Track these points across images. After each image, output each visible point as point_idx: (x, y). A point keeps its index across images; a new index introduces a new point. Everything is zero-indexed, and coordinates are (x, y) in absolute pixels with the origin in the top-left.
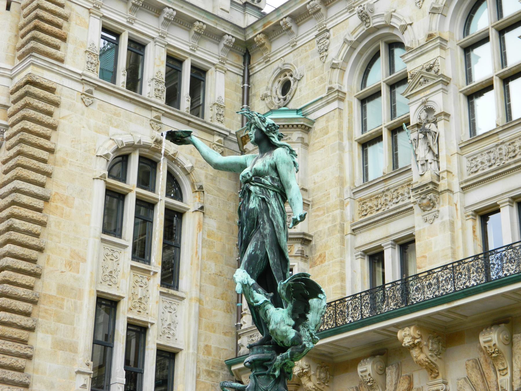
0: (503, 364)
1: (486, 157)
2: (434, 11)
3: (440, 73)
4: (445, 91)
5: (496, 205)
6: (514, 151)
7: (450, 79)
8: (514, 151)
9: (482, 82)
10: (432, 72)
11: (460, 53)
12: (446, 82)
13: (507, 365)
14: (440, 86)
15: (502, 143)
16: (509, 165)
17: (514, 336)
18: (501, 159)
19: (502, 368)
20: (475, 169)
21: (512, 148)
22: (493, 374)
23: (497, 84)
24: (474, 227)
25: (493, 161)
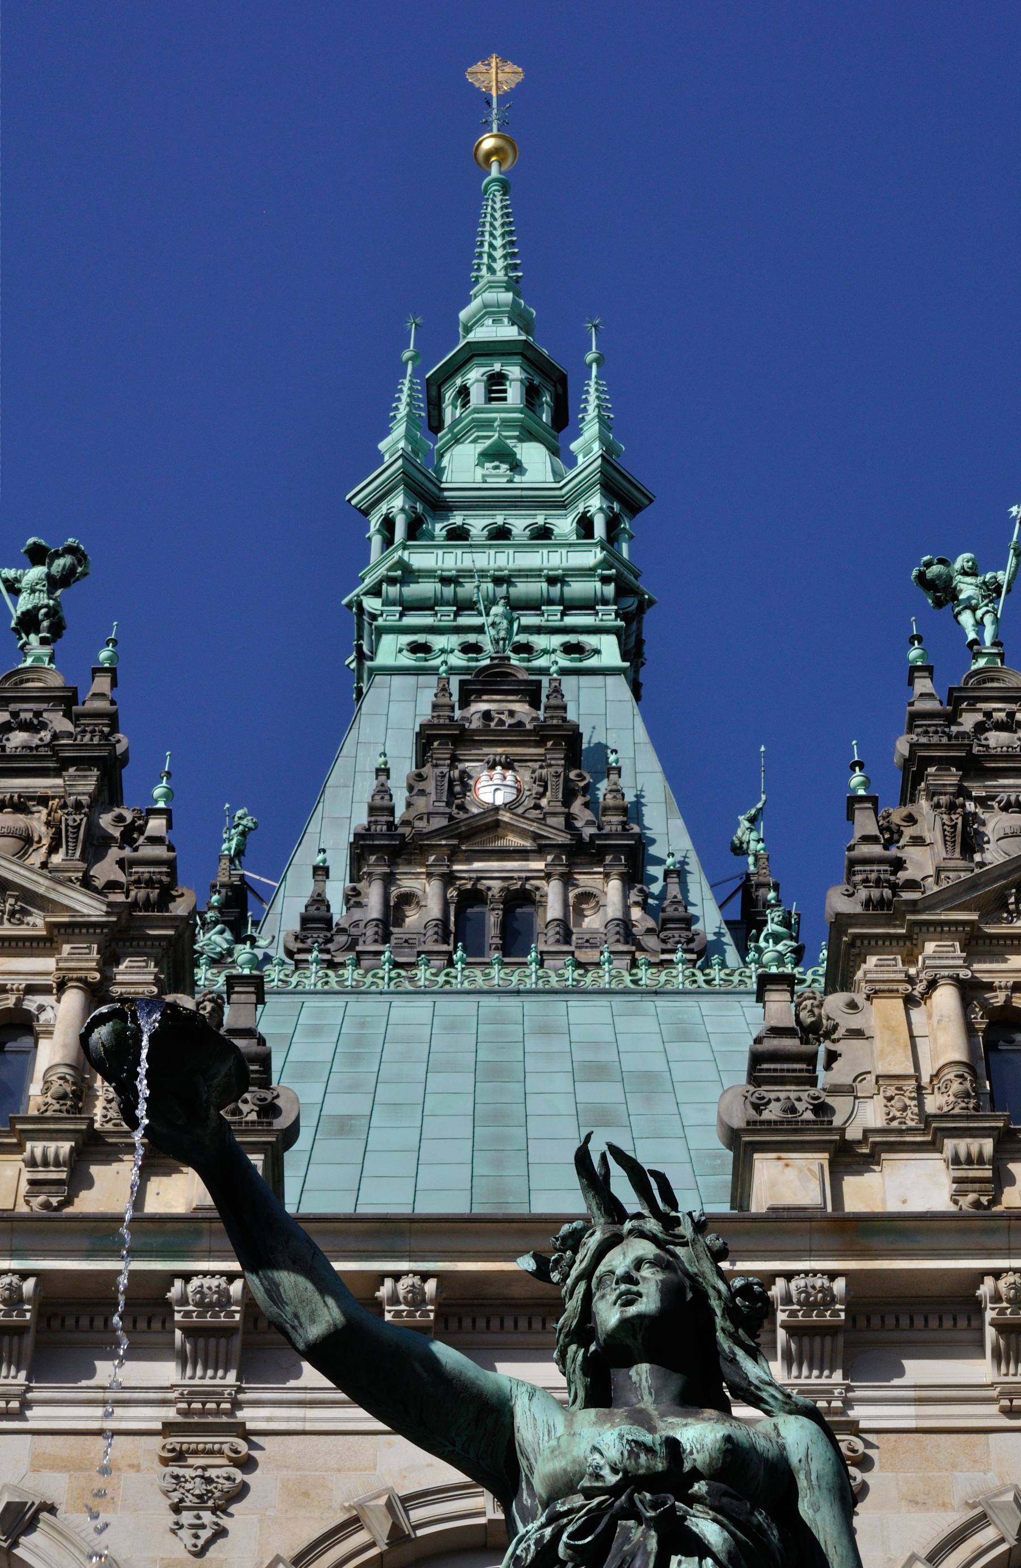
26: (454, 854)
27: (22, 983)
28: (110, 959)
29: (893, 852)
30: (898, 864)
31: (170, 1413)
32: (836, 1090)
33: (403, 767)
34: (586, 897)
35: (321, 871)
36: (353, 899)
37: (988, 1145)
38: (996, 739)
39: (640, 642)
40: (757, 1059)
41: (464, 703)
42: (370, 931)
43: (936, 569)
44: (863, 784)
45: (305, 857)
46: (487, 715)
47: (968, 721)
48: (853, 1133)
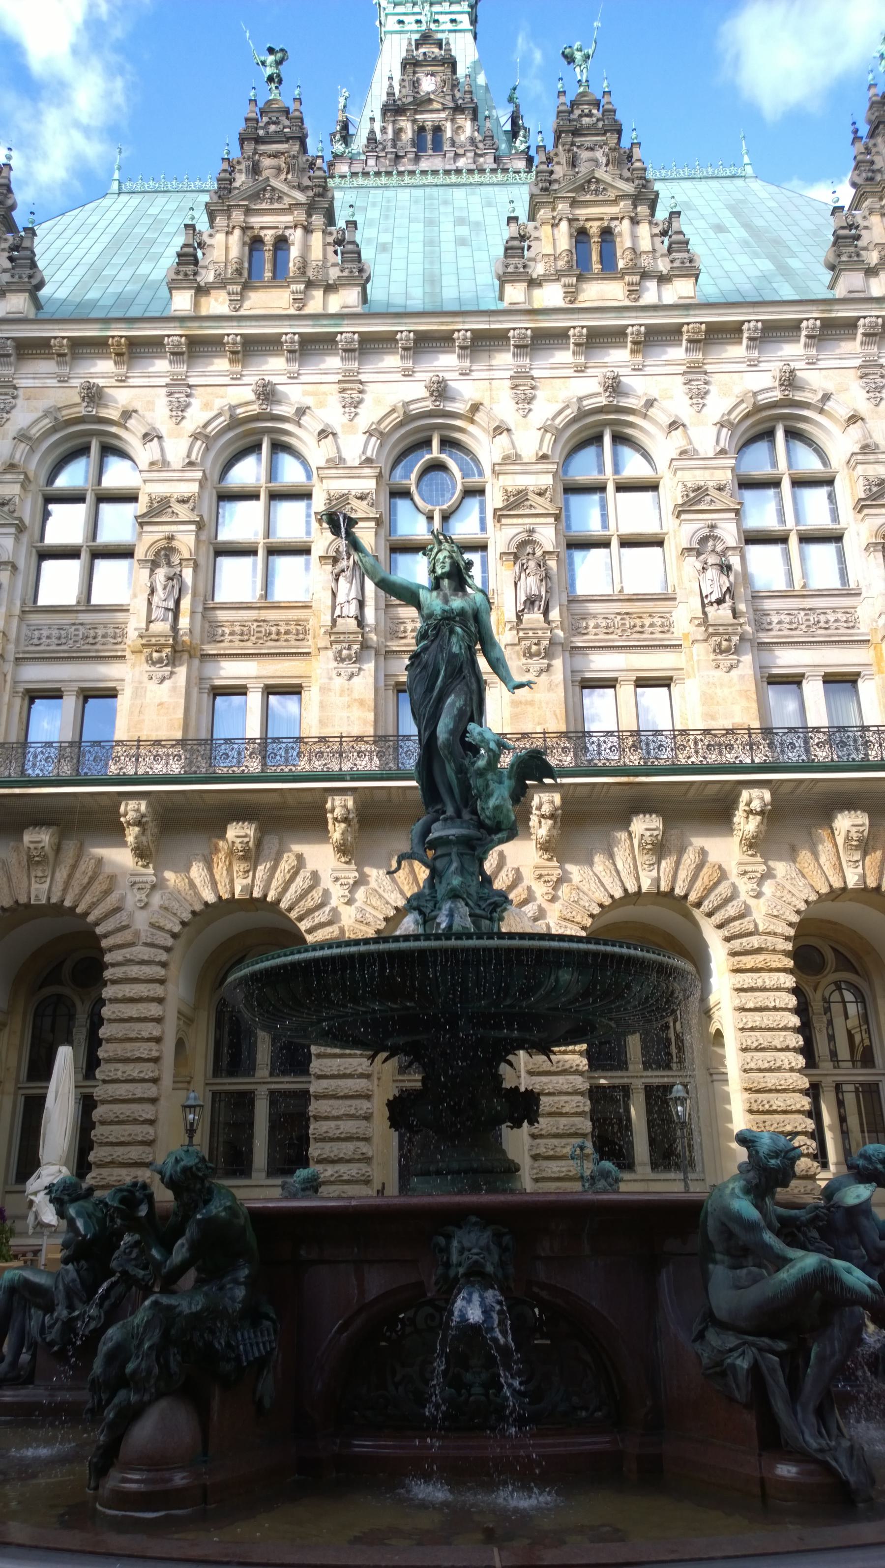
0: (43, 871)
1: (55, 633)
2: (22, 437)
3: (15, 515)
4: (17, 539)
5: (59, 690)
6: (95, 638)
7: (26, 528)
8: (95, 638)
9: (66, 546)
10: (6, 509)
11: (40, 501)
12: (21, 528)
13: (48, 873)
14: (12, 530)
15: (82, 624)
16: (89, 651)
17: (64, 842)
18: (75, 641)
19: (40, 874)
20: (36, 641)
21: (92, 633)
22: (25, 879)
23: (84, 555)
24: (21, 708)
25: (64, 641)
26: (416, 112)
27: (283, 225)
28: (309, 215)
29: (550, 168)
30: (552, 172)
31: (340, 377)
32: (530, 260)
33: (397, 75)
34: (459, 127)
35: (372, 120)
36: (384, 130)
37: (575, 279)
38: (586, 120)
39: (476, 16)
40: (506, 249)
41: (417, 49)
42: (389, 144)
43: (568, 50)
44: (542, 141)
45: (367, 114)
46: (425, 54)
47: (577, 112)
48: (535, 276)
